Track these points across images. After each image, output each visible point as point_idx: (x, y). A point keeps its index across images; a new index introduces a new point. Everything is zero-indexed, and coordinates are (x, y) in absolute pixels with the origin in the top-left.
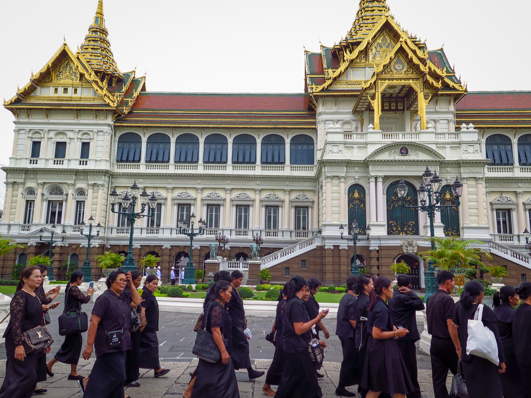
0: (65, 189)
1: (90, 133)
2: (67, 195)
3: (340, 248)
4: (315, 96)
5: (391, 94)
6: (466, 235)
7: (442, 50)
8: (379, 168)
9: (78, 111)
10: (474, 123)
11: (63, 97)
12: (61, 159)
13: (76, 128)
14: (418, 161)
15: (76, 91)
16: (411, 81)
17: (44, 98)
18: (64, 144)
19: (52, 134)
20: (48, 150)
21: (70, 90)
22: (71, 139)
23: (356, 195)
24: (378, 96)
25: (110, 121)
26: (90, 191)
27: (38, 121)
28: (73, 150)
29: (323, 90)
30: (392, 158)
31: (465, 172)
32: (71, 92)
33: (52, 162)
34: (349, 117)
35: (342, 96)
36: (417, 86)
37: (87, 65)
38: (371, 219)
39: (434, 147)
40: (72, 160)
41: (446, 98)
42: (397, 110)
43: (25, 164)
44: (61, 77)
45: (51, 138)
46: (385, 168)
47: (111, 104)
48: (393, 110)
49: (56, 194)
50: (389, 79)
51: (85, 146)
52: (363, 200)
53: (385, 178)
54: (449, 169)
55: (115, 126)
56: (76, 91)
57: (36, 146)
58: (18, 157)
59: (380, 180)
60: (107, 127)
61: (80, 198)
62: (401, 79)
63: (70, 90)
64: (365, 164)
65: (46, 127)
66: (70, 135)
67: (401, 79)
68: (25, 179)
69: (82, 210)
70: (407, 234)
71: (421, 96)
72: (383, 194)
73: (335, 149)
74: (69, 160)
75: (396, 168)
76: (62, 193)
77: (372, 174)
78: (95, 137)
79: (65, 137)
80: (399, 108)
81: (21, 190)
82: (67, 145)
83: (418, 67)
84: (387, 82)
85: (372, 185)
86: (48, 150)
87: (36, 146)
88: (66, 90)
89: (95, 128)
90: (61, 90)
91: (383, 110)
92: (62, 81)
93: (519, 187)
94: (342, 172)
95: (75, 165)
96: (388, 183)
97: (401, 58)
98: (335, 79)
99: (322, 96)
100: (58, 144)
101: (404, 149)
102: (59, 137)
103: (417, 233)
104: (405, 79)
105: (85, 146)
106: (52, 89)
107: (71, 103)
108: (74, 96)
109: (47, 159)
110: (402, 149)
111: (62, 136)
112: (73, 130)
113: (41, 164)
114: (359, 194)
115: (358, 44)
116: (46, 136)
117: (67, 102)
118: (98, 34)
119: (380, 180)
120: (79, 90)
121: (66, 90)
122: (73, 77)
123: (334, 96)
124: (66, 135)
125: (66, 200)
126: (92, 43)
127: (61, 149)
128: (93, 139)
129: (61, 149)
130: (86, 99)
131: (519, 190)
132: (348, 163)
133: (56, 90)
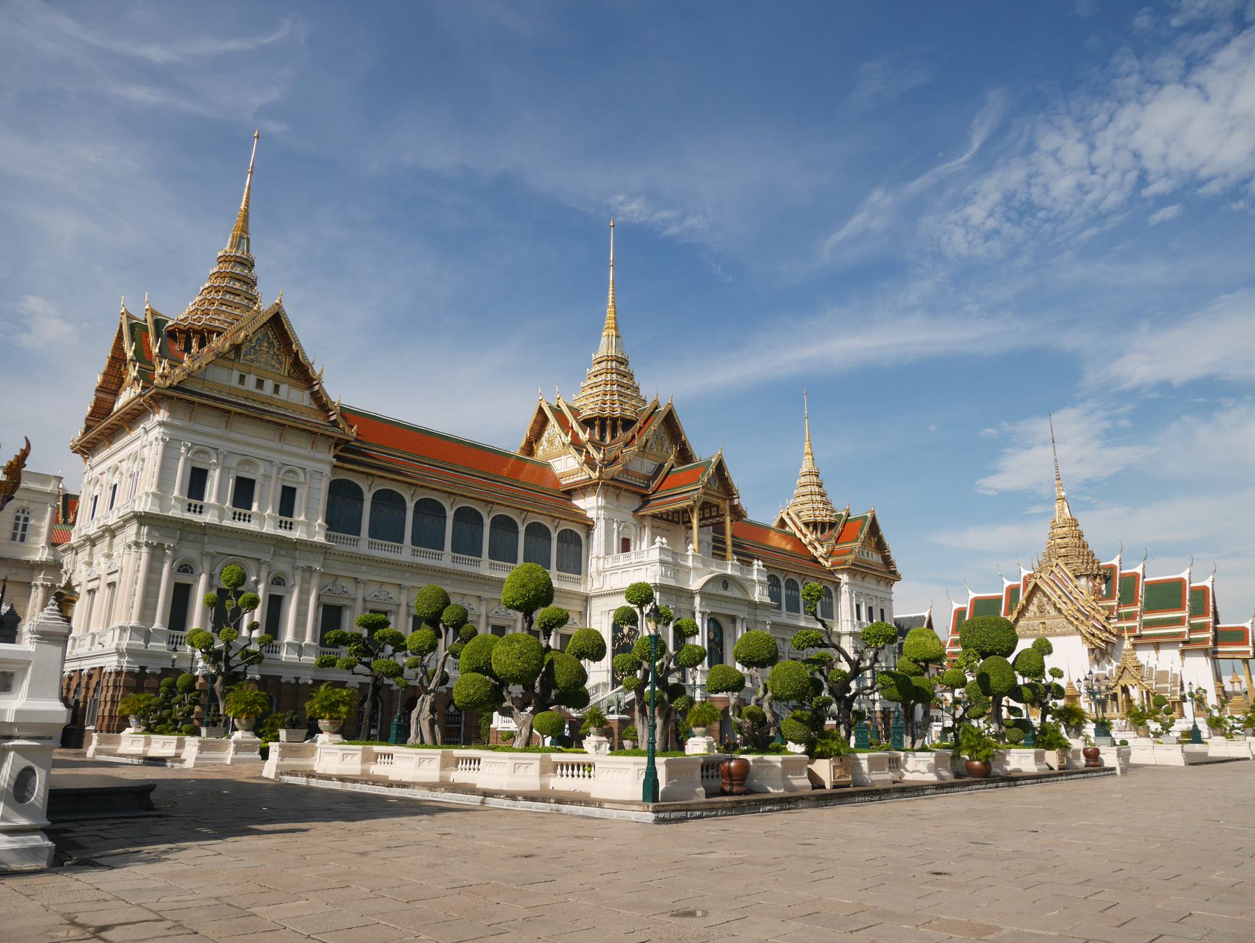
1: (300, 472)
15: (277, 389)
18: (252, 482)
25: (329, 457)
27: (210, 430)
30: (714, 592)
37: (795, 519)
42: (673, 521)
55: (335, 466)
56: (277, 389)
82: (257, 488)
87: (197, 480)
88: (260, 383)
90: (251, 382)
109: (215, 505)
111: (247, 468)
112: (272, 460)
113: (209, 518)
120: (284, 388)
121: (260, 383)
129: (244, 492)
130: (295, 407)
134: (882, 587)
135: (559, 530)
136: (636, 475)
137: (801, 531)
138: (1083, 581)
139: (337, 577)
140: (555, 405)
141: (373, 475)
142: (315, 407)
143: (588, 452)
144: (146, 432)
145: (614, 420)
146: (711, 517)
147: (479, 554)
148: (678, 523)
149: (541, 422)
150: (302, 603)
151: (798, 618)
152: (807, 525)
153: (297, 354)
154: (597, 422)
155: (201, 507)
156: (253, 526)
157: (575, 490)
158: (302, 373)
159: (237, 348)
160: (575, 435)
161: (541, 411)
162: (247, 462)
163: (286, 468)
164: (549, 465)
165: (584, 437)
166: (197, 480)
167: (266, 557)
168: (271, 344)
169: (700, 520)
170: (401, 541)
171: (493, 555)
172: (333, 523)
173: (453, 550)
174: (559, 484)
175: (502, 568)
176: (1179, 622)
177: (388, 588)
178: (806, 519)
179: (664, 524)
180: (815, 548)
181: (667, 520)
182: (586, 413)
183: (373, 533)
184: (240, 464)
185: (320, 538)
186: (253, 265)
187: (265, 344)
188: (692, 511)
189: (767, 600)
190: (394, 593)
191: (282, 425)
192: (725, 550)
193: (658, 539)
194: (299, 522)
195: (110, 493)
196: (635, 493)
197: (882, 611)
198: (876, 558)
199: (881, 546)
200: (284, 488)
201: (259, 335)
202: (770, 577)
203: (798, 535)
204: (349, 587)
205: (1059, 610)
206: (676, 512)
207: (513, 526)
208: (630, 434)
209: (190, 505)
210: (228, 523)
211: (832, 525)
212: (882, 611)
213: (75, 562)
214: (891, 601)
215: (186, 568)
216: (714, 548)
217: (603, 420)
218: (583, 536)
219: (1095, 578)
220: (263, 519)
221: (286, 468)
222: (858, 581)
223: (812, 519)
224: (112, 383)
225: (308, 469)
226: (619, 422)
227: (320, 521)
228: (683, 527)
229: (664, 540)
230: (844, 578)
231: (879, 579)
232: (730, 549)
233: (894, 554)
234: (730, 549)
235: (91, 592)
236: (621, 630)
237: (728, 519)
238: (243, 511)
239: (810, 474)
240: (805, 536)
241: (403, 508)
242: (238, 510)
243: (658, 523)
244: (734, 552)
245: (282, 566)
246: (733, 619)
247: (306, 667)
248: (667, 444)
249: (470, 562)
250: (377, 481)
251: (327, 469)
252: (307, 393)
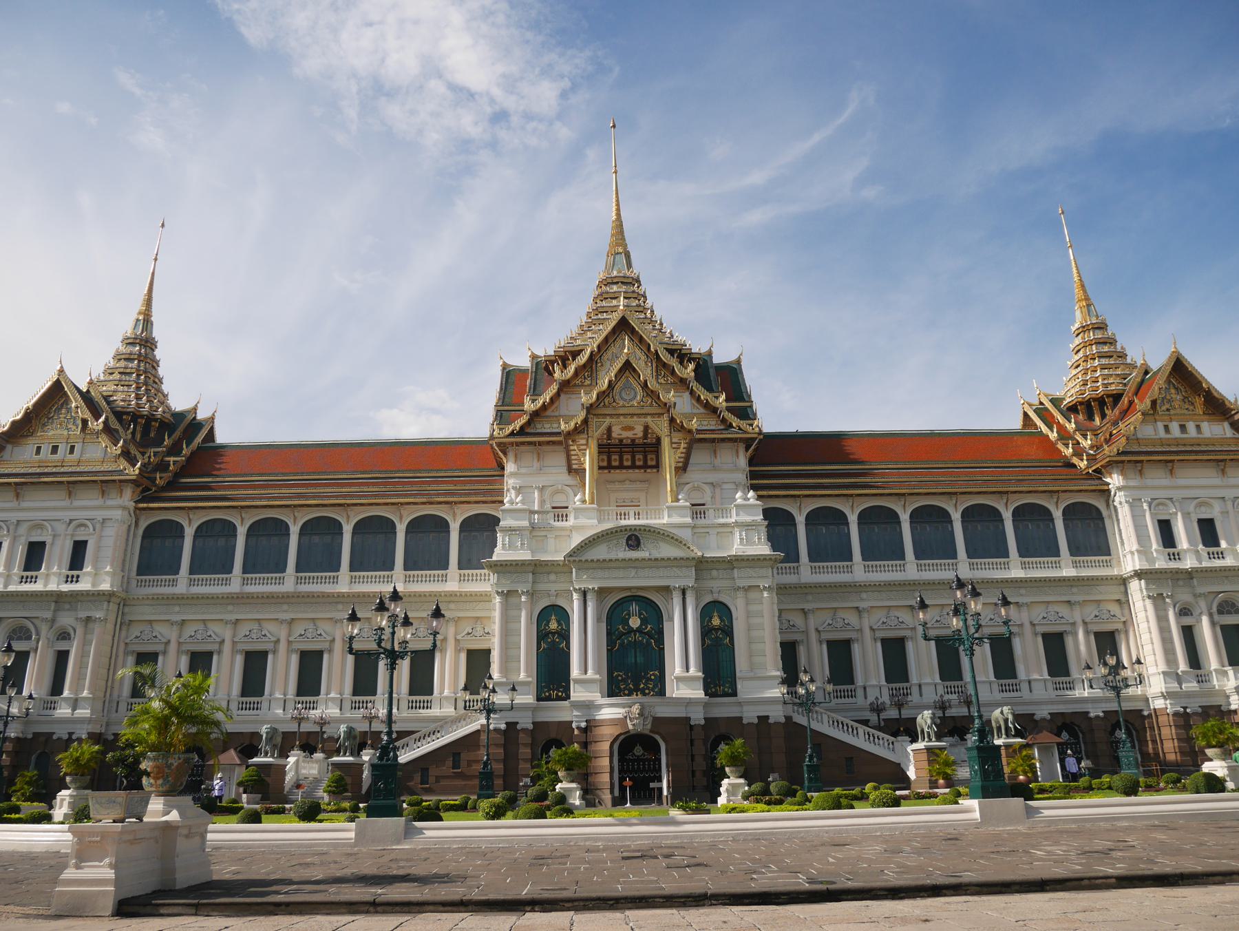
3: (519, 727)
4: (499, 445)
5: (633, 440)
6: (745, 690)
7: (738, 362)
9: (72, 484)
14: (656, 559)
16: (649, 419)
18: (43, 544)
19: (23, 529)
23: (553, 625)
25: (127, 498)
29: (512, 434)
30: (613, 556)
31: (742, 578)
35: (548, 443)
36: (661, 427)
38: (575, 672)
39: (686, 535)
41: (730, 445)
48: (639, 467)
50: (611, 416)
51: (79, 550)
52: (565, 635)
53: (602, 592)
54: (714, 573)
60: (119, 512)
62: (632, 415)
67: (632, 415)
70: (645, 694)
71: (666, 442)
72: (599, 620)
75: (621, 573)
80: (650, 463)
83: (653, 395)
84: (608, 420)
85: (576, 605)
91: (600, 468)
93: (862, 600)
96: (612, 600)
97: (631, 380)
98: (535, 415)
99: (518, 444)
101: (634, 538)
103: (662, 693)
104: (638, 415)
105: (79, 550)
107: (62, 470)
110: (629, 539)
114: (559, 623)
115: (575, 354)
118: (141, 351)
123: (540, 444)
126: (122, 364)
131: (862, 605)
139: (150, 622)
150: (83, 655)
151: (1007, 567)
156: (38, 587)
162: (39, 526)
170: (849, 558)
173: (917, 558)
177: (1057, 608)
183: (919, 555)
189: (764, 549)
190: (1064, 611)
194: (85, 574)
202: (767, 513)
204: (852, 619)
207: (994, 515)
215: (64, 636)
220: (51, 580)
222: (1157, 479)
227: (108, 568)
230: (1114, 480)
239: (1084, 329)
241: (286, 533)
246: (666, 590)
247: (81, 721)
249: (323, 581)
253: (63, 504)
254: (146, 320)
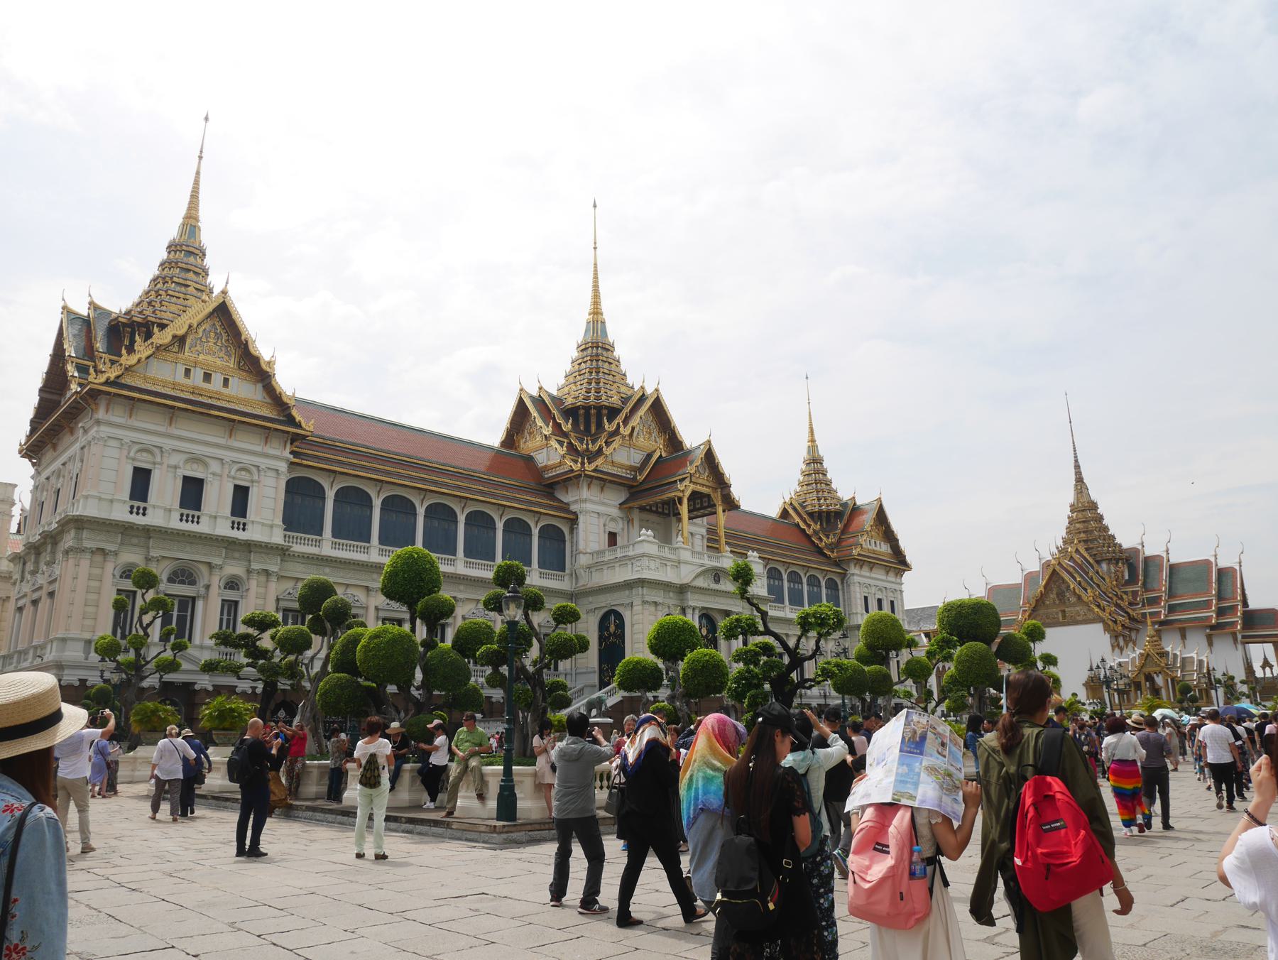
0: (204, 576)
1: (254, 469)
2: (208, 587)
8: (697, 596)
10: (758, 550)
11: (220, 393)
12: (197, 513)
13: (228, 455)
15: (226, 381)
17: (155, 381)
18: (200, 482)
19: (176, 459)
20: (165, 490)
21: (217, 379)
22: (214, 474)
24: (685, 501)
26: (253, 584)
28: (217, 498)
30: (705, 585)
32: (216, 383)
33: (176, 515)
34: (615, 512)
35: (611, 482)
40: (215, 516)
42: (662, 514)
43: (121, 513)
44: (198, 348)
45: (176, 467)
46: (702, 597)
47: (304, 425)
49: (182, 582)
51: (241, 496)
55: (292, 463)
56: (226, 381)
57: (141, 480)
58: (103, 496)
59: (697, 611)
61: (232, 595)
63: (217, 379)
64: (682, 590)
65: (167, 443)
66: (215, 467)
68: (122, 544)
69: (225, 617)
73: (652, 565)
74: (211, 517)
76: (193, 583)
77: (691, 603)
78: (262, 478)
79: (201, 468)
81: (110, 567)
86: (165, 490)
87: (141, 480)
88: (207, 377)
89: (264, 463)
90: (198, 375)
92: (201, 357)
94: (659, 596)
95: (224, 529)
100: (186, 479)
102: (188, 466)
105: (241, 496)
106: (181, 370)
108: (224, 390)
111: (195, 466)
113: (154, 518)
116: (166, 461)
117: (209, 401)
118: (185, 258)
119: (697, 611)
121: (207, 377)
122: (221, 355)
124: (206, 465)
125: (206, 597)
127: (192, 492)
128: (258, 482)
129: (192, 492)
132: (665, 586)
133: (187, 372)
134: (891, 577)
135: (539, 526)
136: (621, 466)
137: (805, 521)
138: (1104, 566)
140: (535, 393)
141: (335, 472)
142: (268, 400)
143: (570, 444)
144: (86, 431)
145: (599, 408)
146: (705, 508)
147: (454, 553)
148: (668, 515)
149: (521, 416)
152: (811, 514)
153: (246, 345)
154: (581, 412)
155: (145, 509)
156: (204, 527)
157: (557, 483)
158: (257, 370)
159: (180, 340)
160: (557, 426)
161: (521, 403)
162: (195, 459)
163: (237, 466)
164: (532, 458)
165: (567, 427)
166: (141, 482)
167: (216, 561)
168: (218, 336)
169: (690, 511)
171: (468, 553)
172: (291, 522)
174: (542, 477)
175: (479, 567)
176: (1207, 605)
178: (809, 508)
179: (653, 518)
180: (821, 539)
181: (656, 512)
182: (569, 401)
184: (187, 461)
185: (277, 537)
186: (204, 255)
187: (212, 335)
188: (681, 503)
191: (232, 421)
192: (717, 541)
193: (644, 531)
195: (54, 497)
196: (620, 484)
197: (892, 602)
198: (884, 548)
199: (889, 536)
200: (236, 487)
201: (206, 326)
203: (803, 526)
205: (1079, 597)
206: (664, 503)
208: (616, 422)
209: (132, 507)
210: (175, 523)
211: (839, 515)
212: (892, 602)
213: (23, 572)
214: (901, 592)
216: (709, 540)
217: (587, 408)
218: (566, 531)
219: (1117, 561)
221: (237, 466)
223: (817, 508)
224: (55, 381)
225: (263, 466)
226: (605, 412)
228: (674, 519)
229: (650, 532)
231: (888, 570)
232: (723, 540)
233: (903, 544)
234: (723, 540)
235: (35, 603)
236: (607, 629)
237: (720, 509)
238: (191, 512)
240: (809, 526)
242: (186, 512)
243: (646, 516)
244: (727, 543)
245: (234, 569)
248: (655, 433)
250: (339, 478)
251: (283, 467)
252: (260, 386)
253: (222, 441)
254: (191, 224)
